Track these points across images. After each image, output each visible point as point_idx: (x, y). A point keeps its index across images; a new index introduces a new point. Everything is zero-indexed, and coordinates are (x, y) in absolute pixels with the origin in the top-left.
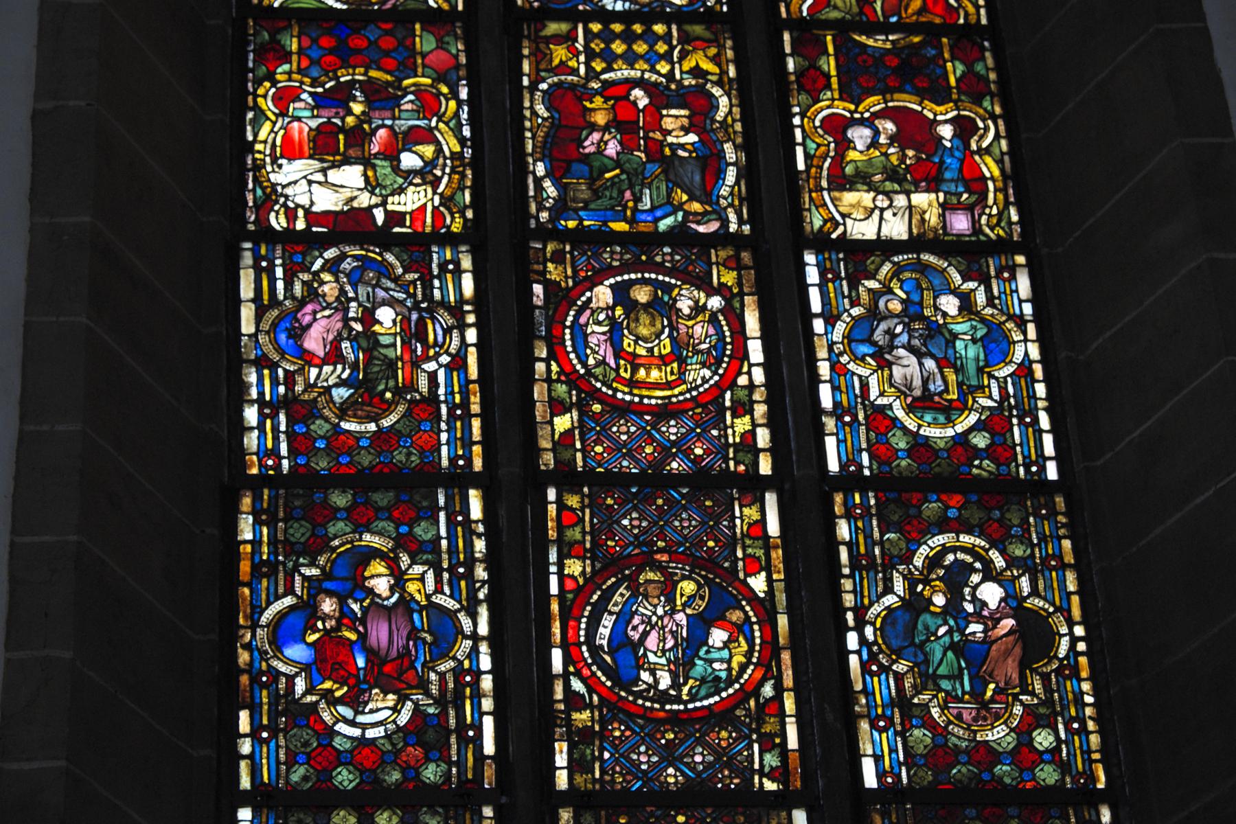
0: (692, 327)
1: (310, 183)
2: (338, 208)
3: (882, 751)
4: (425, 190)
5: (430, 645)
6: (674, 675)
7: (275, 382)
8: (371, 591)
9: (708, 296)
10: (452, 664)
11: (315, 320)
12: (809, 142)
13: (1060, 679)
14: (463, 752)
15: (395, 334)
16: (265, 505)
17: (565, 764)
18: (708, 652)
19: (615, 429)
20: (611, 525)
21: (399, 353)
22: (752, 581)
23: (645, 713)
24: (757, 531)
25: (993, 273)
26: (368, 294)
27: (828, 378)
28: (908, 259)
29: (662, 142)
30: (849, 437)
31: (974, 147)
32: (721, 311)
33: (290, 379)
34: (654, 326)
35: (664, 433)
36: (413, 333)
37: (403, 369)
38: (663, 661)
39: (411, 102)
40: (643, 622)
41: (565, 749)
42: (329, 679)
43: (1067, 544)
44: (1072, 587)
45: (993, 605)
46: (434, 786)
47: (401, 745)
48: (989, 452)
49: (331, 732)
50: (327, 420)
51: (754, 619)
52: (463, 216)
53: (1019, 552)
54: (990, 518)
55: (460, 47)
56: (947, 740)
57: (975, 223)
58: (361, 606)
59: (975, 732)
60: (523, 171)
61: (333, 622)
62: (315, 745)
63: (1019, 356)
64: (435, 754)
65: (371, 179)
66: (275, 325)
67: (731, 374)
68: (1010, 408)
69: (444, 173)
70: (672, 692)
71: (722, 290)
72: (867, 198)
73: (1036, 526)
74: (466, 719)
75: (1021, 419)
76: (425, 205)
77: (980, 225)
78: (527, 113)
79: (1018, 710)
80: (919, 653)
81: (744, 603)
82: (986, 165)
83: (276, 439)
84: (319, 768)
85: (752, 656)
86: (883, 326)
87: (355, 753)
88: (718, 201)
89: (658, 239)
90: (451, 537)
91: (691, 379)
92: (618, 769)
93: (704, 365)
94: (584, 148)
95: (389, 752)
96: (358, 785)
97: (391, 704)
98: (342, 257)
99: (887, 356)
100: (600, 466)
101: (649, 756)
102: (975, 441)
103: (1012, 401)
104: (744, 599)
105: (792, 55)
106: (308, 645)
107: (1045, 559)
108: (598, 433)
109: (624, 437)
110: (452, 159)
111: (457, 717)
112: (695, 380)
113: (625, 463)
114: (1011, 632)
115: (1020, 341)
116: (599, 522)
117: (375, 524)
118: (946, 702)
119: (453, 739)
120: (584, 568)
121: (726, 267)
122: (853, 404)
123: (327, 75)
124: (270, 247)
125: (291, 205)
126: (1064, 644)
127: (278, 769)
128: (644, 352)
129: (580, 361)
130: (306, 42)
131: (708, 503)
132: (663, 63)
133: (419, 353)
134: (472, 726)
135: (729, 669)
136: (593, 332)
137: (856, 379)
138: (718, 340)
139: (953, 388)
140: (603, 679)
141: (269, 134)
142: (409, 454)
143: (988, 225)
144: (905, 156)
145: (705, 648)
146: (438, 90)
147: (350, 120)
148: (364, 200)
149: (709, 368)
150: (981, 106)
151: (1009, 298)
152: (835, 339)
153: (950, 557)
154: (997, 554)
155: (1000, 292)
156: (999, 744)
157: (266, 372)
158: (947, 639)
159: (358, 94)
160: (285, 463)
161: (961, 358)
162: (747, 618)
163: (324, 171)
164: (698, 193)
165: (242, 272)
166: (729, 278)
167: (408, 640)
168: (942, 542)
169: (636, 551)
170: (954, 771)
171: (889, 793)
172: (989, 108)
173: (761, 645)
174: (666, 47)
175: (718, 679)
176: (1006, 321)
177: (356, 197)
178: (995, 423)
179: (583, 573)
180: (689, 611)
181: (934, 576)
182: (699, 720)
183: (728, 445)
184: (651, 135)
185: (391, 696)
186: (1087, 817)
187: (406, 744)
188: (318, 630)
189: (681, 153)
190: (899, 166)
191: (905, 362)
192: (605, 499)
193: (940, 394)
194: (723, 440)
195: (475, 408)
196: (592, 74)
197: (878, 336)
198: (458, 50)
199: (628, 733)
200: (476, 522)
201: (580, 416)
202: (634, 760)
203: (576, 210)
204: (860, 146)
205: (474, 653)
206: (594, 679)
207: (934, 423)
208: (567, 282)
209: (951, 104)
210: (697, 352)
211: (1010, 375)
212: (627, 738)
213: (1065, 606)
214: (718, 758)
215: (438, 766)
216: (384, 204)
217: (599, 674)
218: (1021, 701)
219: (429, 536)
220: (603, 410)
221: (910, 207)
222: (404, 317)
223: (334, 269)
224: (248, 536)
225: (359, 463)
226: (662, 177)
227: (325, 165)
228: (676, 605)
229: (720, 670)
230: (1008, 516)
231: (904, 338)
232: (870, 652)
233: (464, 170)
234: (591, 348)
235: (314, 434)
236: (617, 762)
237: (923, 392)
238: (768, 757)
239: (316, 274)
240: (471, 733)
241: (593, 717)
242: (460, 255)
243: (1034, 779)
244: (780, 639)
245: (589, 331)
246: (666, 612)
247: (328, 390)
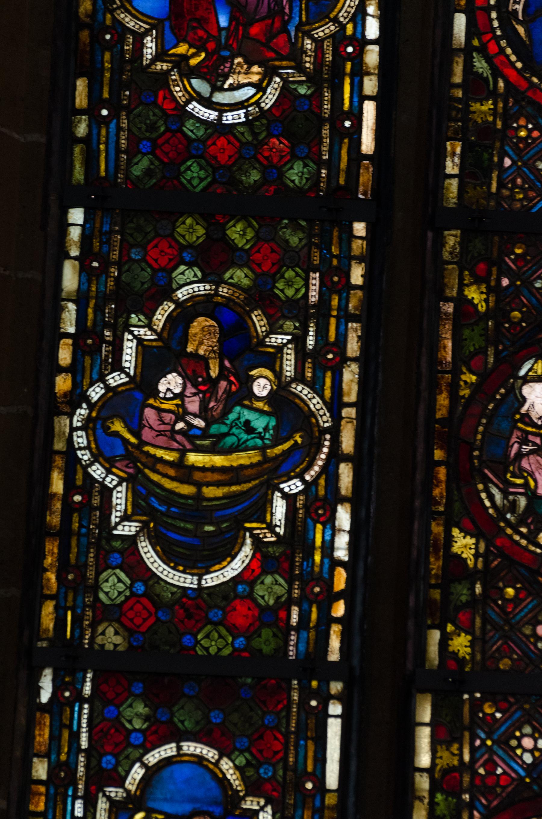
14: (336, 147)
17: (456, 171)
41: (458, 150)
42: (185, 41)
46: (299, 190)
47: (264, 134)
62: (162, 129)
64: (303, 150)
74: (343, 104)
84: (166, 160)
87: (209, 142)
92: (519, 181)
95: (248, 143)
96: (210, 184)
97: (255, 78)
111: (333, 102)
119: (326, 132)
134: (348, 115)
140: (513, 58)
185: (256, 69)
187: (270, 135)
199: (536, 134)
206: (502, 58)
212: (535, 140)
215: (305, 165)
217: (509, 51)
236: (519, 172)
240: (347, 124)
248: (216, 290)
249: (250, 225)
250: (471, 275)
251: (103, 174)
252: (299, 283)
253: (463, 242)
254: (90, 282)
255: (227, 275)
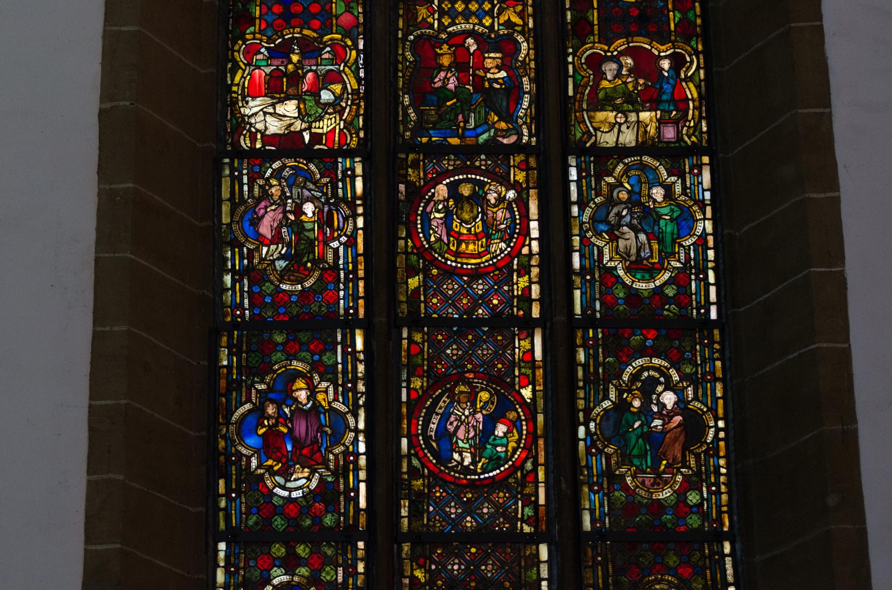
0: (496, 213)
1: (265, 114)
2: (281, 132)
3: (595, 506)
4: (335, 117)
5: (330, 435)
6: (473, 456)
7: (242, 258)
8: (296, 400)
9: (507, 190)
10: (342, 448)
11: (266, 212)
12: (577, 74)
13: (707, 457)
14: (347, 506)
15: (314, 222)
16: (235, 342)
17: (406, 514)
18: (494, 440)
19: (445, 287)
20: (439, 354)
21: (316, 235)
22: (523, 391)
23: (456, 482)
24: (528, 357)
25: (687, 170)
26: (298, 193)
27: (578, 248)
28: (635, 160)
29: (483, 78)
30: (588, 290)
31: (683, 76)
32: (514, 200)
33: (250, 257)
34: (472, 212)
35: (474, 289)
36: (324, 220)
37: (318, 246)
38: (467, 446)
39: (328, 52)
40: (456, 420)
41: (407, 504)
42: (271, 458)
43: (718, 364)
44: (719, 394)
45: (669, 407)
46: (330, 528)
48: (675, 300)
49: (272, 494)
50: (272, 283)
51: (523, 418)
52: (358, 136)
53: (688, 370)
54: (672, 347)
55: (360, 10)
56: (634, 499)
57: (679, 133)
58: (290, 409)
59: (652, 493)
60: (397, 102)
61: (274, 421)
63: (699, 230)
64: (331, 508)
65: (303, 110)
66: (242, 217)
67: (518, 246)
68: (691, 267)
69: (347, 105)
70: (472, 467)
71: (515, 186)
72: (611, 116)
73: (700, 352)
74: (349, 485)
75: (697, 275)
76: (335, 128)
77: (682, 135)
78: (400, 58)
79: (679, 478)
80: (622, 440)
81: (517, 406)
82: (689, 89)
83: (242, 296)
85: (520, 443)
86: (615, 210)
87: (285, 507)
88: (517, 120)
89: (478, 149)
90: (345, 362)
91: (493, 250)
92: (437, 517)
93: (502, 240)
94: (435, 83)
95: (304, 506)
96: (286, 527)
97: (306, 475)
98: (284, 167)
99: (616, 233)
100: (435, 313)
101: (457, 509)
102: (667, 291)
103: (692, 263)
104: (517, 404)
105: (569, 9)
106: (259, 436)
107: (704, 374)
108: (435, 290)
109: (450, 292)
110: (352, 94)
112: (496, 251)
113: (450, 311)
114: (679, 425)
115: (700, 220)
116: (433, 351)
117: (299, 354)
118: (635, 473)
119: (342, 499)
120: (423, 383)
121: (519, 169)
122: (592, 266)
123: (276, 34)
124: (240, 161)
125: (253, 130)
126: (712, 432)
127: (241, 517)
128: (465, 232)
129: (426, 240)
130: (265, 10)
131: (499, 338)
132: (487, 18)
133: (328, 235)
135: (506, 451)
136: (435, 218)
137: (595, 248)
138: (512, 222)
139: (656, 254)
140: (431, 458)
141: (241, 79)
142: (320, 306)
143: (687, 135)
144: (638, 83)
145: (493, 437)
146: (345, 43)
147: (290, 67)
148: (298, 126)
149: (505, 242)
150: (689, 45)
151: (696, 188)
152: (584, 220)
153: (646, 374)
154: (675, 372)
155: (691, 184)
156: (666, 501)
157: (237, 250)
158: (639, 430)
159: (296, 47)
160: (247, 312)
161: (662, 232)
162: (519, 416)
163: (273, 105)
164: (504, 115)
165: (223, 179)
166: (521, 177)
167: (317, 432)
168: (641, 363)
169: (454, 372)
170: (638, 519)
171: (598, 533)
172: (695, 46)
173: (526, 435)
174: (490, 6)
175: (499, 458)
176: (693, 205)
177: (293, 124)
178: (680, 280)
179: (422, 387)
180: (484, 412)
181: (635, 387)
182: (487, 485)
183: (513, 297)
184: (477, 72)
185: (306, 470)
186: (716, 549)
187: (315, 502)
188: (265, 426)
189: (497, 86)
190: (633, 91)
191: (627, 236)
192: (437, 336)
193: (647, 259)
194: (511, 294)
195: (361, 273)
196: (442, 28)
197: (612, 217)
198: (359, 13)
199: (444, 494)
200: (359, 352)
201: (424, 278)
202: (447, 512)
203: (428, 130)
204: (609, 77)
205: (356, 440)
206: (426, 458)
207: (643, 279)
208: (420, 182)
209: (670, 44)
210: (498, 231)
211: (692, 244)
212: (444, 497)
213: (714, 407)
214: (497, 511)
215: (333, 515)
216: (310, 128)
217: (429, 455)
218: (681, 472)
219: (331, 362)
220: (438, 273)
221: (638, 122)
222: (320, 209)
223: (279, 176)
224: (225, 363)
225: (291, 313)
226: (482, 104)
227: (274, 101)
228: (476, 408)
229: (501, 452)
230: (684, 344)
231: (628, 219)
232: (592, 440)
233: (360, 102)
234: (433, 229)
235: (264, 293)
237: (637, 258)
238: (527, 509)
239: (268, 179)
240: (352, 494)
241: (424, 483)
242: (355, 164)
243: (686, 525)
244: (538, 431)
245: (432, 217)
246: (470, 413)
247: (273, 261)
248: (292, 579)
249: (307, 546)
250: (417, 564)
251: (234, 525)
252: (333, 573)
253: (412, 549)
254: (230, 578)
255: (297, 571)
